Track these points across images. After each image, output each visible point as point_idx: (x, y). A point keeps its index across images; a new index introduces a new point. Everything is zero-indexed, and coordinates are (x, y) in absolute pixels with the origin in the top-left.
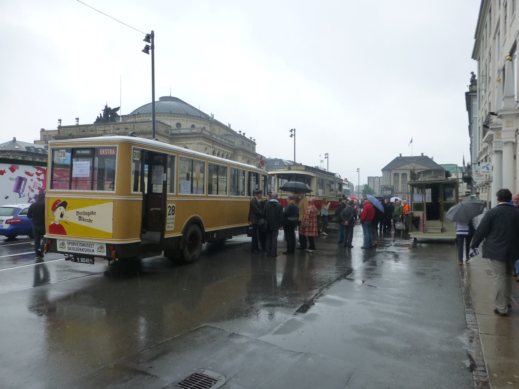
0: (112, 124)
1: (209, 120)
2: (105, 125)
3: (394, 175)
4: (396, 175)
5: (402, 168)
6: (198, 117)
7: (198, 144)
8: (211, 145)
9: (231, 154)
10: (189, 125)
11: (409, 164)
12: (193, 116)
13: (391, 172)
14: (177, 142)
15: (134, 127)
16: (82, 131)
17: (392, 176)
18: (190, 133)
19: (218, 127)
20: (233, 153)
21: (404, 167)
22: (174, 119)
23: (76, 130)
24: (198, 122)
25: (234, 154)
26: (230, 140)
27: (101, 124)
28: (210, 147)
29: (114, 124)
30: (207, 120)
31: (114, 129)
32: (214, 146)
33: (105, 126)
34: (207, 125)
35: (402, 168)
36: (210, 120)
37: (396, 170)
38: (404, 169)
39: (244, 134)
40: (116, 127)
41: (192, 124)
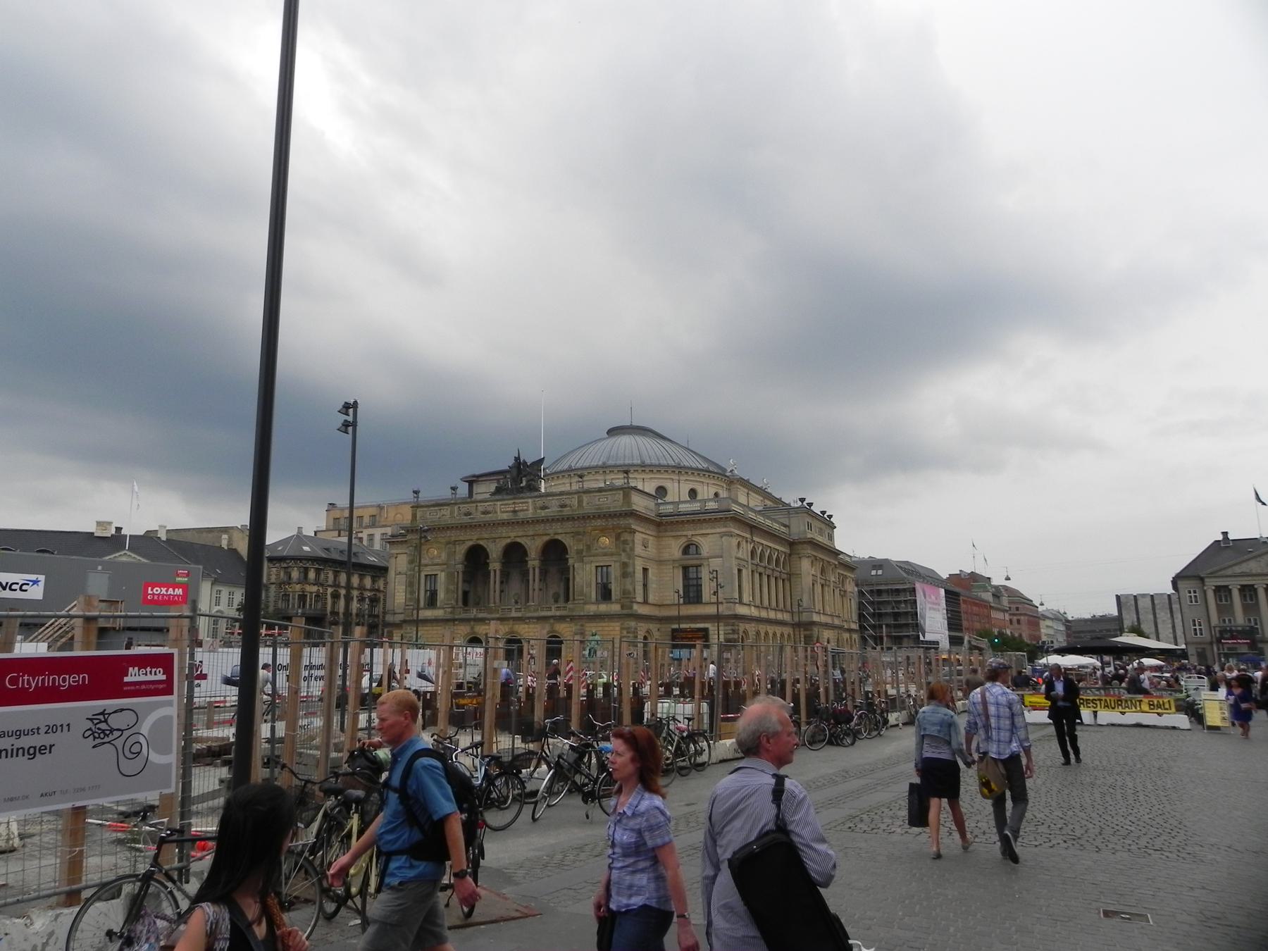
0: (531, 498)
1: (726, 476)
2: (515, 498)
3: (1214, 591)
4: (1222, 592)
5: (1237, 570)
6: (702, 470)
7: (723, 535)
8: (748, 536)
9: (785, 553)
10: (686, 488)
11: (1258, 559)
12: (691, 468)
13: (1206, 584)
14: (672, 531)
15: (580, 502)
16: (466, 515)
17: (1210, 595)
18: (703, 511)
19: (746, 491)
20: (788, 551)
21: (1244, 568)
22: (651, 478)
23: (452, 513)
24: (703, 482)
25: (790, 555)
26: (780, 520)
27: (505, 497)
28: (747, 542)
29: (536, 497)
30: (720, 474)
31: (535, 508)
32: (755, 539)
33: (516, 501)
34: (723, 487)
35: (1237, 570)
36: (728, 474)
37: (1222, 577)
38: (1243, 575)
39: (810, 504)
40: (540, 502)
41: (691, 487)
